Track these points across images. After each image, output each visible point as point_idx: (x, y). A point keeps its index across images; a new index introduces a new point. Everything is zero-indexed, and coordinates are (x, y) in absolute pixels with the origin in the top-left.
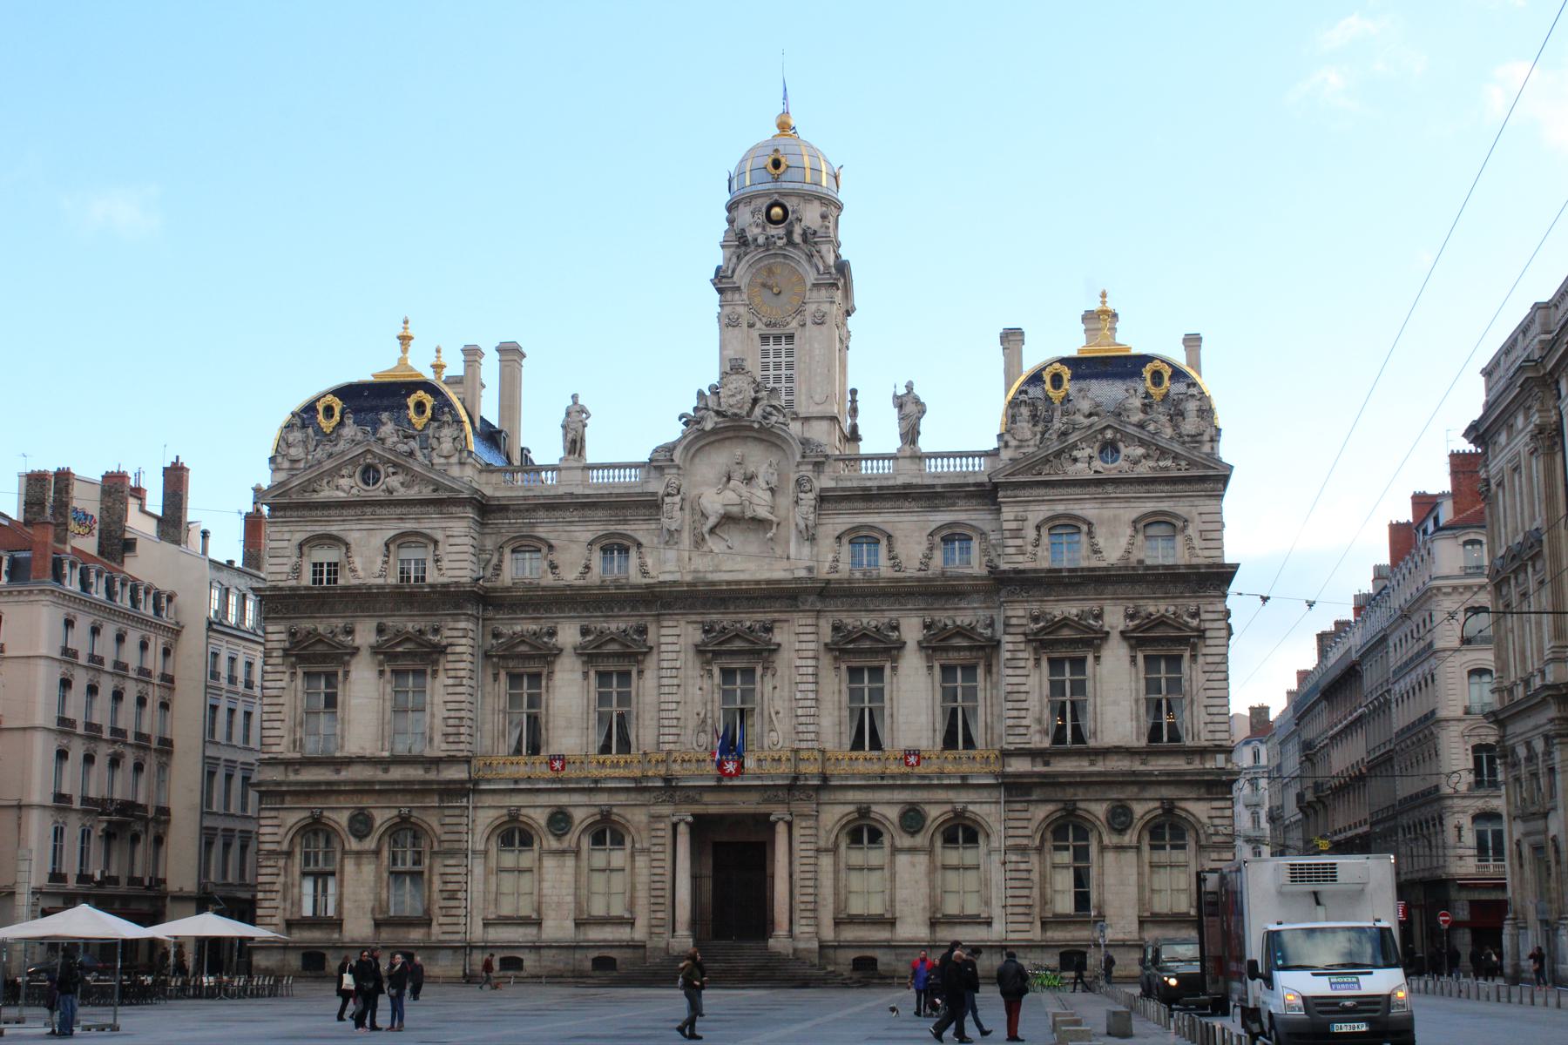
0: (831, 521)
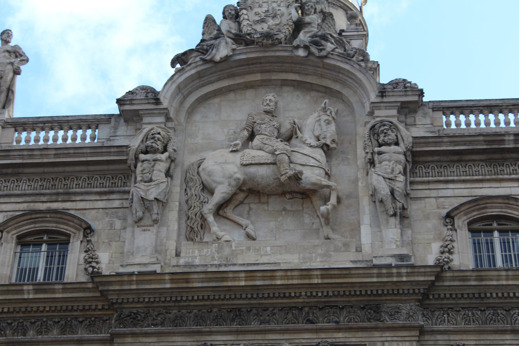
0: (434, 193)
